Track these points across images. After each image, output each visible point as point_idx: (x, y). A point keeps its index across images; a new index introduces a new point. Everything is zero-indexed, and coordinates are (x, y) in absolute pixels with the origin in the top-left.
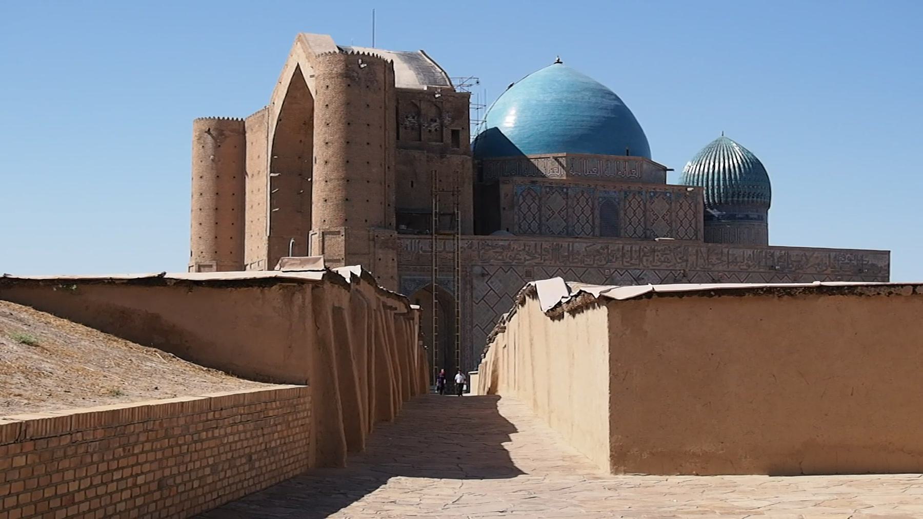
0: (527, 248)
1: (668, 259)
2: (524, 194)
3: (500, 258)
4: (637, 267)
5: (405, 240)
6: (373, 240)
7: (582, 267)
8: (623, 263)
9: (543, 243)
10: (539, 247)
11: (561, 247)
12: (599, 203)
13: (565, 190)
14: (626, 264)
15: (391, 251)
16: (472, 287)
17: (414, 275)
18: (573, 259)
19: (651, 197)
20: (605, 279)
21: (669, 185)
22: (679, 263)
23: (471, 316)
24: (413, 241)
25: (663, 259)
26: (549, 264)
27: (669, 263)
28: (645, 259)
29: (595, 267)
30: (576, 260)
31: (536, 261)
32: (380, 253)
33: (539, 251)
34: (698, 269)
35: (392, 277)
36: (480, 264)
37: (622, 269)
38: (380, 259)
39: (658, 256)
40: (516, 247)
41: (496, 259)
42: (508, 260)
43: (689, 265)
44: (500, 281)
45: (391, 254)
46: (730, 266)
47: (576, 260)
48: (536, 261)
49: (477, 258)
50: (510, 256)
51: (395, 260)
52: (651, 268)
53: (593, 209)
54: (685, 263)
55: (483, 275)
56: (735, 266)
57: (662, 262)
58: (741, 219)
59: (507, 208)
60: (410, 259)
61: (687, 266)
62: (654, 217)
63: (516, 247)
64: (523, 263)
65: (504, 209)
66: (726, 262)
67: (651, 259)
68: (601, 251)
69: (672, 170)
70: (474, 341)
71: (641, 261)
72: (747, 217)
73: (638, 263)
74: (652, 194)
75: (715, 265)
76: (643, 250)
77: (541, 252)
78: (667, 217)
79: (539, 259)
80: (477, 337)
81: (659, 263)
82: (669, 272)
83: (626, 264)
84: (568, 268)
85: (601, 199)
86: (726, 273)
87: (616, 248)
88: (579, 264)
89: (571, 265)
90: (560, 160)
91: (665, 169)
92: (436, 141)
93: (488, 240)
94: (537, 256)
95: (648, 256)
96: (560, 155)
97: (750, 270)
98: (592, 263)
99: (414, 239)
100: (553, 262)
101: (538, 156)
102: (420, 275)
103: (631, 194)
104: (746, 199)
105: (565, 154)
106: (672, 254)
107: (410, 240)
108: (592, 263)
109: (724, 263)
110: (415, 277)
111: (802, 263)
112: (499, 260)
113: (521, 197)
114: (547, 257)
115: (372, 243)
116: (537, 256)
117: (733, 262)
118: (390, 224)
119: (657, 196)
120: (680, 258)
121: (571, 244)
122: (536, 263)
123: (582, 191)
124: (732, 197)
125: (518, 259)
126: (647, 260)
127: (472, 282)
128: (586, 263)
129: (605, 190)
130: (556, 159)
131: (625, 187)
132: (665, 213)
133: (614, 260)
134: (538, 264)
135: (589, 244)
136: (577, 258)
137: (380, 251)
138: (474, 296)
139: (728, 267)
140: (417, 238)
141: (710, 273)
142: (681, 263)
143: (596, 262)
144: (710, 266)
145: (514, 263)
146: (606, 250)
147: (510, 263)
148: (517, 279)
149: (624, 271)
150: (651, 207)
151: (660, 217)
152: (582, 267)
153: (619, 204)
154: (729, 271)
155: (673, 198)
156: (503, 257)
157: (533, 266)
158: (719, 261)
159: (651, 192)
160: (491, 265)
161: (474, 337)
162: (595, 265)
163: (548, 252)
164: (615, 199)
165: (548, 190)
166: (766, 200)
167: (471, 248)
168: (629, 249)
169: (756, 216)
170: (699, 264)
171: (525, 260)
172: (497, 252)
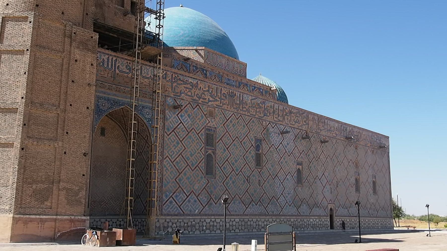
0: (211, 90)
3: (190, 94)
4: (281, 123)
5: (102, 55)
6: (70, 37)
9: (223, 89)
10: (219, 91)
11: (235, 95)
13: (205, 72)
14: (275, 119)
15: (90, 54)
16: (164, 117)
17: (109, 94)
23: (163, 147)
24: (110, 58)
26: (226, 108)
28: (286, 117)
29: (257, 118)
30: (245, 109)
31: (218, 103)
32: (77, 54)
33: (219, 95)
36: (172, 96)
37: (273, 123)
38: (76, 61)
39: (293, 117)
41: (187, 95)
44: (189, 116)
47: (245, 109)
48: (218, 103)
49: (170, 90)
51: (95, 65)
52: (289, 125)
55: (175, 107)
60: (106, 76)
68: (261, 105)
70: (165, 173)
71: (284, 119)
73: (282, 120)
77: (221, 96)
79: (219, 102)
80: (167, 169)
81: (294, 123)
83: (275, 119)
84: (239, 115)
87: (270, 105)
90: (200, 52)
93: (180, 75)
94: (218, 99)
95: (288, 116)
96: (200, 48)
98: (255, 114)
99: (111, 55)
100: (229, 107)
101: (183, 48)
102: (115, 95)
103: (242, 85)
105: (204, 48)
106: (301, 117)
107: (107, 56)
108: (255, 114)
110: (110, 96)
111: (359, 137)
115: (67, 40)
116: (218, 99)
117: (329, 130)
119: (256, 90)
121: (241, 94)
122: (217, 105)
123: (215, 75)
127: (165, 112)
128: (251, 113)
129: (228, 78)
130: (196, 50)
131: (239, 79)
135: (253, 98)
136: (245, 108)
137: (77, 51)
138: (166, 127)
140: (115, 56)
143: (257, 114)
145: (200, 102)
146: (264, 105)
147: (197, 100)
148: (202, 118)
149: (275, 124)
156: (192, 94)
157: (214, 108)
160: (181, 99)
161: (165, 169)
162: (257, 116)
163: (226, 97)
167: (166, 78)
168: (277, 108)
171: (209, 101)
172: (187, 88)
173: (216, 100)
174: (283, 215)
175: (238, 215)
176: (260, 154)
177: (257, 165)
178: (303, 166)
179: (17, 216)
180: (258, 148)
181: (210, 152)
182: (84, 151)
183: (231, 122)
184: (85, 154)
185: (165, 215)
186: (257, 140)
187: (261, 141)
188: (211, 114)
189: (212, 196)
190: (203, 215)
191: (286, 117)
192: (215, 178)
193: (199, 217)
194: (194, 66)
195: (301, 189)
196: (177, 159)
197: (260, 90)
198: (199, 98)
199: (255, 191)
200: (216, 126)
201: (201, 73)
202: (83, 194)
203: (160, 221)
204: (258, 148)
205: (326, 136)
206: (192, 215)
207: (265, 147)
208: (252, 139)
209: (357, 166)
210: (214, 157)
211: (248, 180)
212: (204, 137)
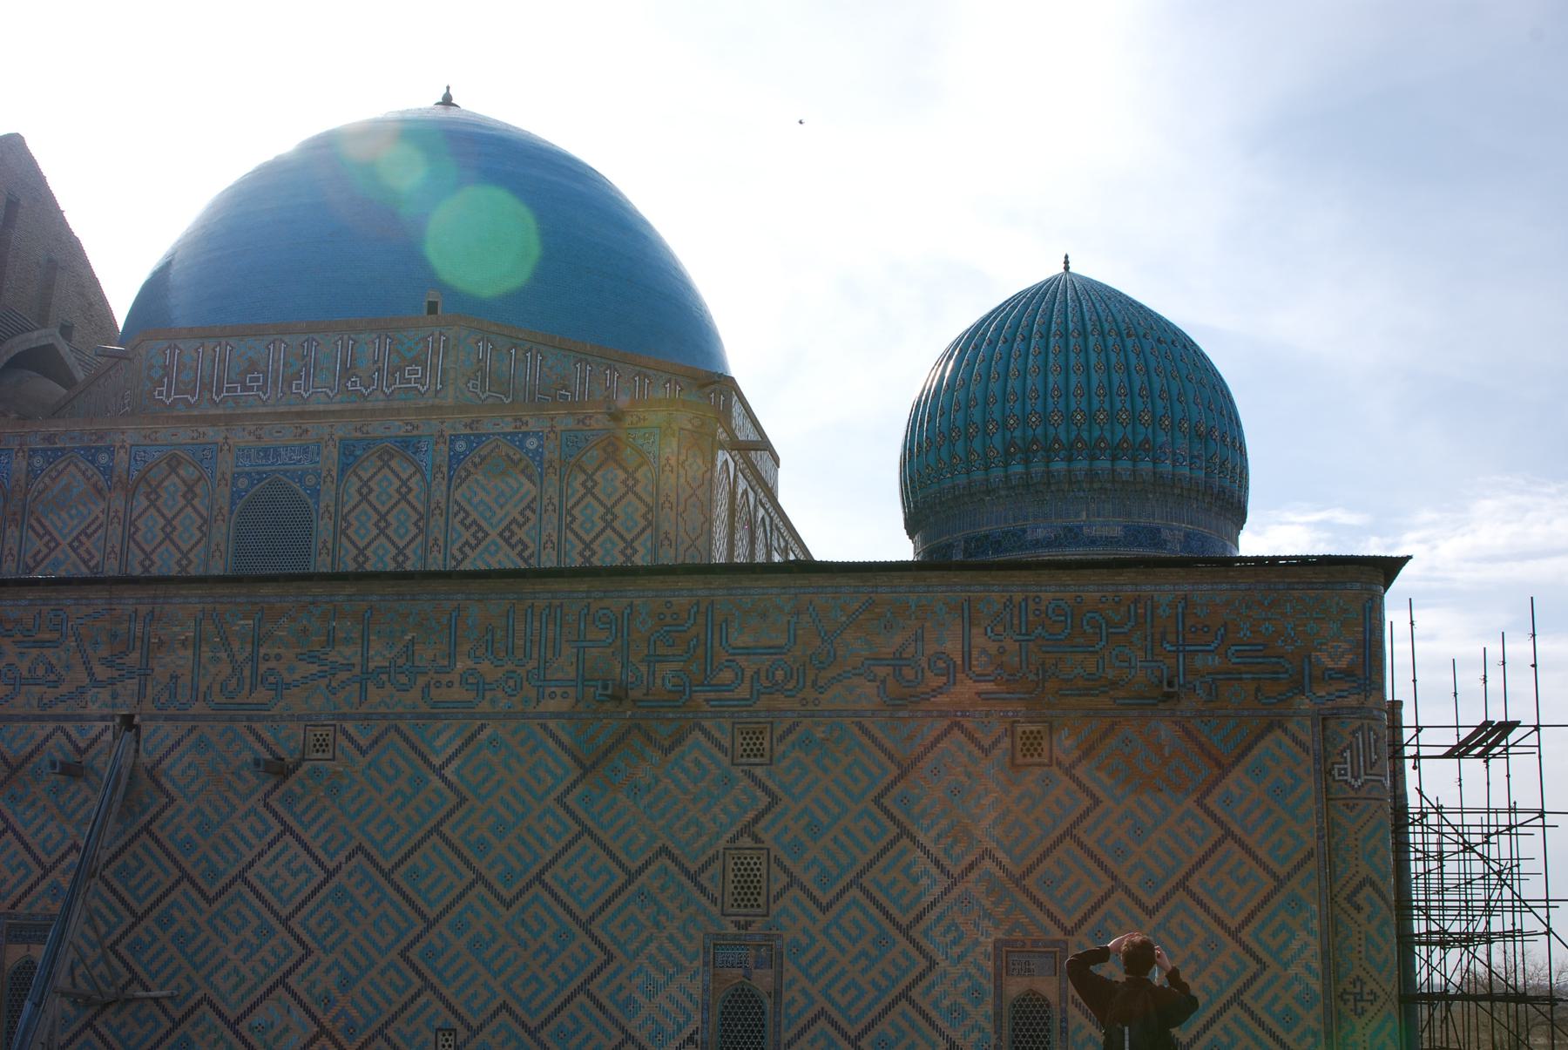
1: (51, 668)
13: (103, 459)
19: (455, 459)
22: (97, 683)
34: (198, 708)
46: (371, 688)
54: (132, 685)
56: (404, 689)
61: (141, 695)
62: (467, 535)
66: (357, 670)
74: (461, 446)
75: (288, 686)
78: (521, 534)
82: (50, 726)
97: (485, 706)
104: (1059, 466)
109: (344, 675)
120: (108, 663)
124: (1006, 465)
132: (515, 514)
139: (364, 690)
141: (257, 726)
142: (112, 682)
151: (493, 533)
153: (316, 493)
154: (367, 717)
158: (314, 668)
159: (455, 438)
165: (38, 462)
166: (1161, 468)
169: (1117, 532)
170: (203, 688)
194: (35, 451)
197: (522, 447)
201: (84, 474)
205: (344, 717)
209: (748, 889)
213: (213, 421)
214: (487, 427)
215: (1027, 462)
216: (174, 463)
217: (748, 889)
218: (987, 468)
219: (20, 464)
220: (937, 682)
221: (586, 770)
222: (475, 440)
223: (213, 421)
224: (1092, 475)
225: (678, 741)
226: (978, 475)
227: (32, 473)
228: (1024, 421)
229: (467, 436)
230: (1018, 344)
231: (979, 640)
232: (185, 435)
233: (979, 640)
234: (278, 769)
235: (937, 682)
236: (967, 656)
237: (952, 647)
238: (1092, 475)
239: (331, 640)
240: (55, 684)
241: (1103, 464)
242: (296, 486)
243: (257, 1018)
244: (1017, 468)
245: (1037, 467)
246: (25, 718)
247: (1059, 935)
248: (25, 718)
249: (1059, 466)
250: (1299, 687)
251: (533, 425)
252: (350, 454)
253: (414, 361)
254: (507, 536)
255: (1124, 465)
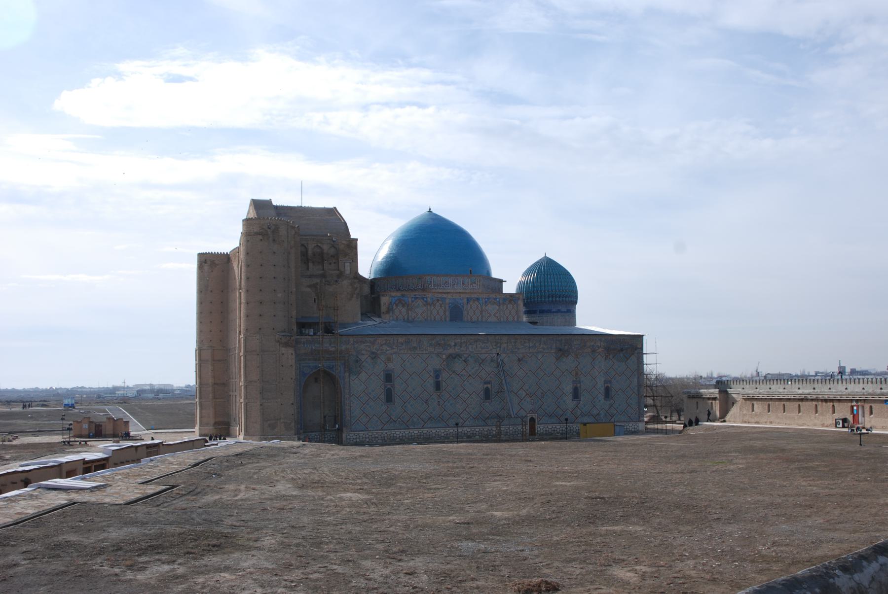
2: (397, 303)
3: (369, 349)
7: (426, 354)
8: (455, 349)
10: (396, 341)
12: (449, 307)
13: (425, 299)
18: (420, 348)
19: (486, 302)
20: (442, 361)
21: (505, 294)
22: (494, 349)
25: (483, 346)
27: (488, 348)
31: (395, 350)
32: (283, 350)
34: (508, 352)
35: (291, 365)
38: (283, 354)
40: (380, 342)
42: (374, 351)
43: (501, 350)
45: (291, 351)
48: (395, 350)
50: (376, 348)
51: (294, 354)
52: (475, 352)
53: (445, 312)
54: (499, 349)
57: (482, 348)
58: (554, 312)
59: (385, 312)
63: (380, 342)
64: (385, 352)
65: (383, 313)
67: (474, 347)
69: (505, 281)
70: (352, 405)
72: (559, 311)
74: (486, 300)
76: (469, 341)
81: (480, 349)
82: (487, 355)
83: (457, 350)
85: (450, 305)
86: (528, 354)
88: (424, 352)
89: (419, 352)
91: (501, 281)
92: (335, 270)
98: (433, 350)
104: (558, 299)
108: (433, 350)
112: (369, 351)
113: (394, 305)
114: (401, 348)
116: (395, 347)
118: (293, 330)
120: (495, 345)
124: (549, 298)
125: (382, 350)
126: (472, 347)
133: (449, 348)
134: (395, 353)
137: (283, 349)
141: (516, 354)
142: (496, 348)
144: (516, 350)
150: (487, 308)
152: (426, 354)
153: (463, 307)
155: (501, 302)
157: (392, 354)
159: (486, 298)
161: (352, 403)
162: (436, 352)
164: (460, 305)
165: (413, 299)
169: (566, 310)
173: (394, 349)
174: (466, 427)
175: (417, 428)
176: (439, 381)
177: (436, 390)
178: (493, 384)
179: (262, 437)
180: (437, 376)
181: (389, 387)
182: (291, 402)
183: (408, 361)
184: (292, 404)
185: (354, 431)
186: (435, 371)
187: (440, 371)
188: (389, 360)
189: (391, 416)
190: (385, 430)
191: (471, 346)
192: (394, 404)
193: (381, 431)
195: (490, 404)
196: (361, 396)
198: (378, 351)
199: (434, 410)
200: (393, 367)
202: (293, 424)
203: (350, 435)
204: (437, 376)
206: (375, 430)
207: (444, 375)
208: (431, 372)
209: (576, 374)
210: (392, 389)
211: (426, 402)
212: (383, 377)
213: (444, 293)
214: (491, 296)
215: (552, 298)
216: (438, 300)
217: (576, 374)
218: (545, 298)
219: (410, 300)
220: (597, 349)
221: (557, 360)
222: (489, 299)
223: (444, 293)
224: (562, 300)
225: (568, 356)
226: (543, 299)
227: (412, 301)
228: (552, 291)
229: (487, 298)
230: (549, 276)
231: (602, 343)
232: (440, 295)
233: (602, 343)
234: (519, 360)
235: (597, 349)
236: (601, 345)
237: (599, 344)
238: (562, 300)
239: (525, 343)
240: (488, 348)
241: (564, 299)
242: (459, 305)
243: (519, 393)
244: (551, 299)
245: (554, 299)
246: (484, 353)
247: (610, 379)
248: (484, 353)
249: (558, 299)
250: (636, 350)
251: (498, 297)
252: (468, 299)
253: (474, 283)
254: (494, 315)
255: (567, 299)
